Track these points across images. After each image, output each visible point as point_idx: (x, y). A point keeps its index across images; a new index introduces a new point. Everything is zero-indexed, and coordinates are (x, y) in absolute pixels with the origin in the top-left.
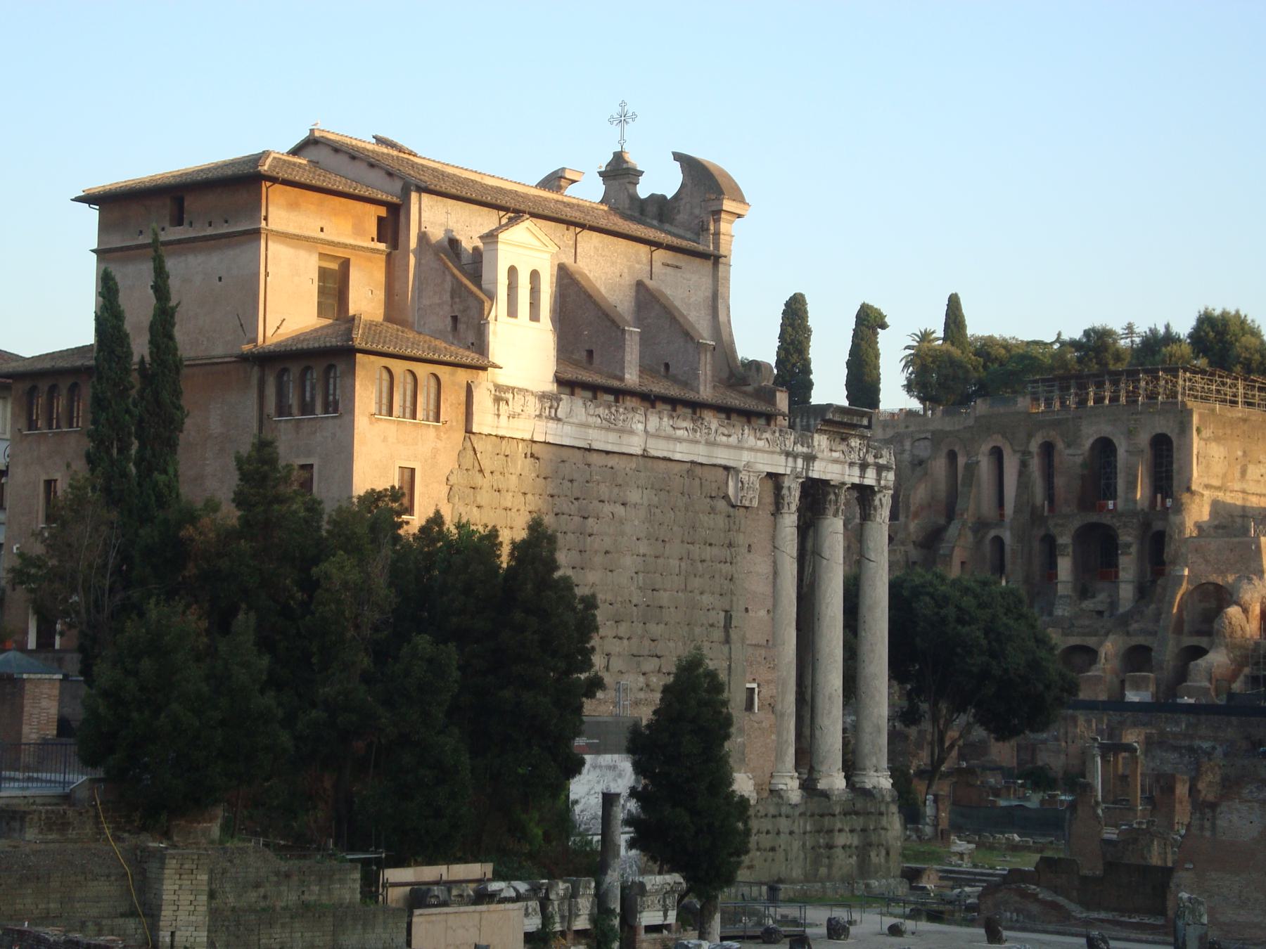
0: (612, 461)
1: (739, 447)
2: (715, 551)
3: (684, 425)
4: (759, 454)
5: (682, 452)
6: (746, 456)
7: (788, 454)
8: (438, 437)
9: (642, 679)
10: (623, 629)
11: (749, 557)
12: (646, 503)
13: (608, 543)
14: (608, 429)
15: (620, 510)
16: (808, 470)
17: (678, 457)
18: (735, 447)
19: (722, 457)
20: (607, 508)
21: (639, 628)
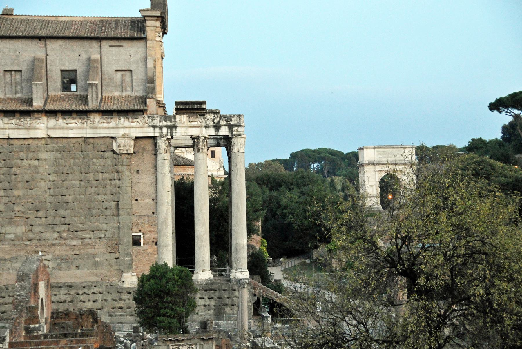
0: (26, 142)
2: (105, 175)
4: (132, 129)
6: (122, 131)
7: (154, 127)
9: (56, 235)
10: (40, 214)
11: (137, 176)
12: (53, 158)
13: (27, 177)
14: (18, 129)
15: (36, 163)
16: (172, 132)
18: (113, 128)
20: (25, 162)
21: (52, 213)
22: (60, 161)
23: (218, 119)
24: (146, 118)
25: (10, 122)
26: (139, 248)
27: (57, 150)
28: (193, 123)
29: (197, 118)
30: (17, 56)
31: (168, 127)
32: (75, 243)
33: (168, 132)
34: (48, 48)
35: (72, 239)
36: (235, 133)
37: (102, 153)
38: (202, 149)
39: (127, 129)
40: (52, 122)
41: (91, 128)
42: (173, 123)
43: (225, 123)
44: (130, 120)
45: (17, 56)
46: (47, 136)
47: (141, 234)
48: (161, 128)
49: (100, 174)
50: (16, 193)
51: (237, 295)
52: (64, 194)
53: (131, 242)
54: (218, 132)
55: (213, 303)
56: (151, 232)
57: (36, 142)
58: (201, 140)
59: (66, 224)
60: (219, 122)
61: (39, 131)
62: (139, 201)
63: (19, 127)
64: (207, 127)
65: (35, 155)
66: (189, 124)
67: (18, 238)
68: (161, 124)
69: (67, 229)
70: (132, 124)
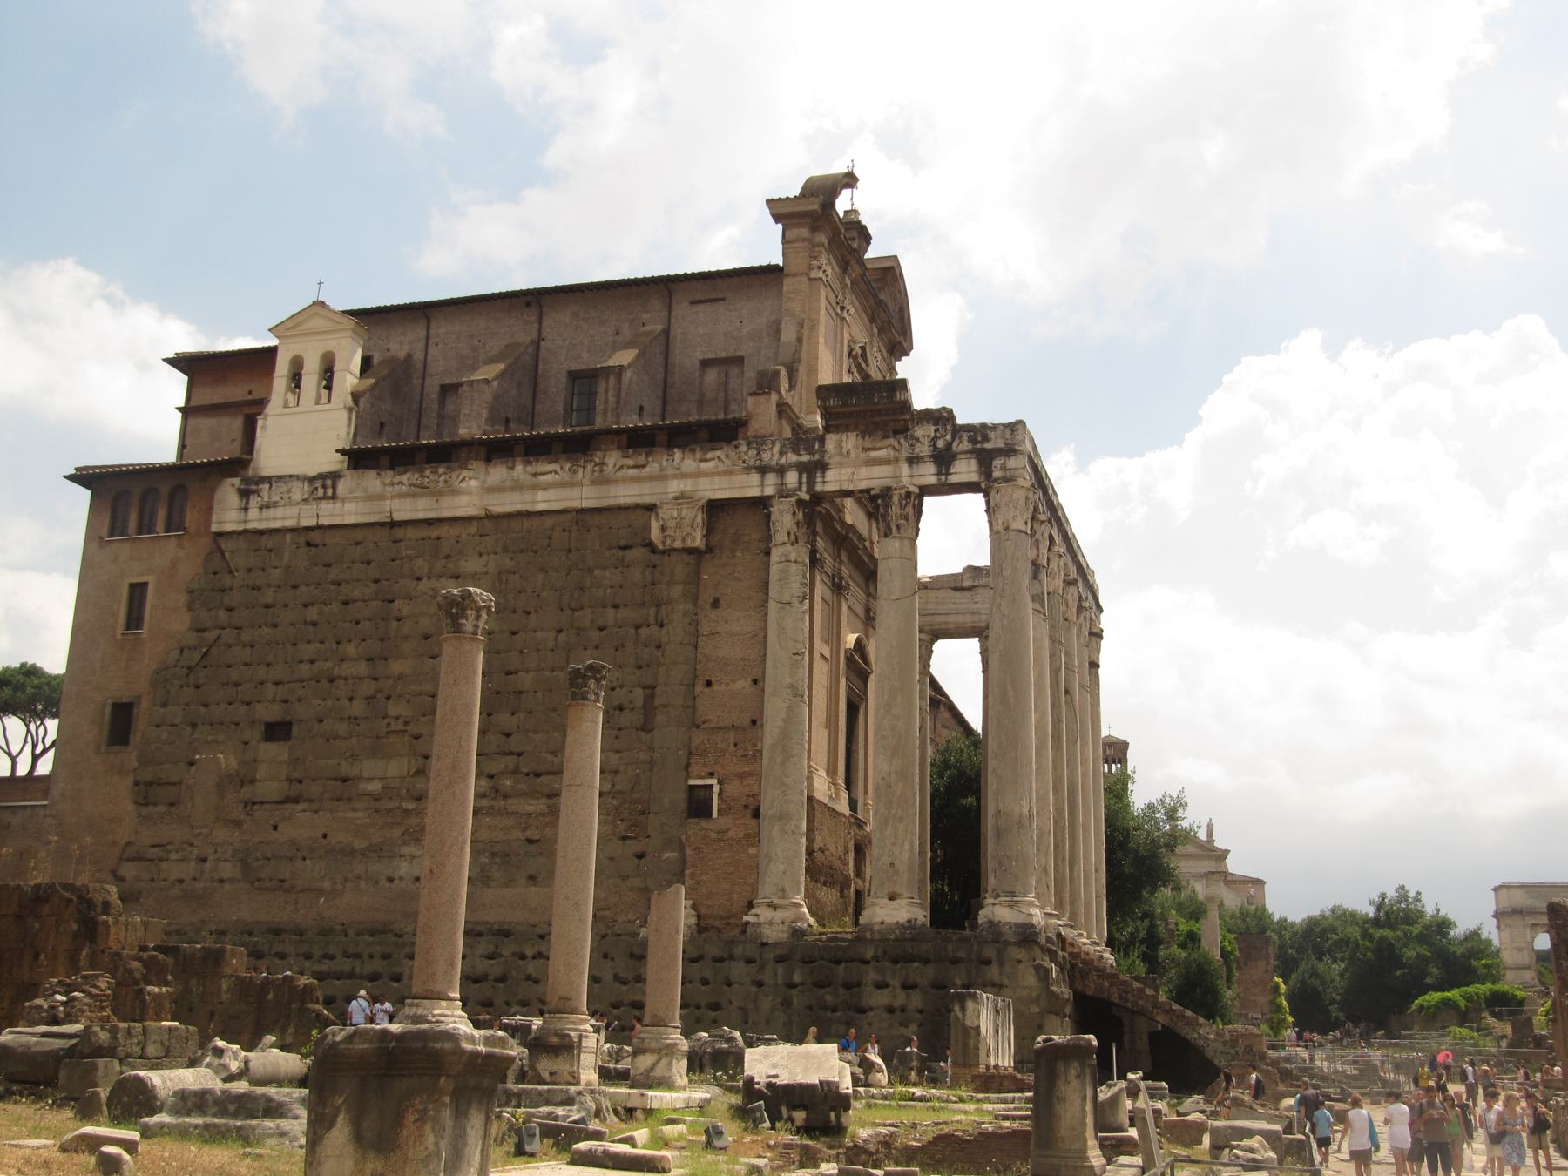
1: (662, 477)
2: (624, 613)
3: (552, 471)
5: (544, 501)
6: (675, 487)
7: (763, 470)
8: (180, 546)
11: (713, 614)
12: (492, 568)
14: (414, 495)
16: (811, 483)
17: (541, 507)
18: (651, 478)
19: (626, 494)
22: (511, 577)
23: (949, 437)
24: (744, 448)
25: (397, 479)
26: (704, 824)
27: (506, 550)
28: (873, 454)
29: (886, 437)
30: (474, 349)
31: (800, 468)
32: (530, 809)
33: (800, 483)
34: (545, 323)
35: (523, 794)
36: (997, 474)
37: (621, 553)
38: (898, 527)
39: (689, 481)
40: (498, 473)
41: (593, 482)
42: (817, 457)
43: (966, 446)
44: (698, 455)
45: (474, 349)
46: (483, 513)
47: (713, 781)
48: (781, 471)
49: (611, 611)
50: (396, 667)
51: (996, 978)
52: (512, 668)
53: (684, 806)
54: (948, 474)
55: (916, 1001)
56: (741, 776)
57: (453, 531)
58: (896, 499)
59: (511, 753)
60: (949, 445)
61: (464, 500)
62: (715, 687)
63: (420, 490)
64: (913, 461)
65: (451, 566)
66: (863, 455)
67: (388, 792)
68: (783, 461)
69: (512, 767)
70: (703, 465)
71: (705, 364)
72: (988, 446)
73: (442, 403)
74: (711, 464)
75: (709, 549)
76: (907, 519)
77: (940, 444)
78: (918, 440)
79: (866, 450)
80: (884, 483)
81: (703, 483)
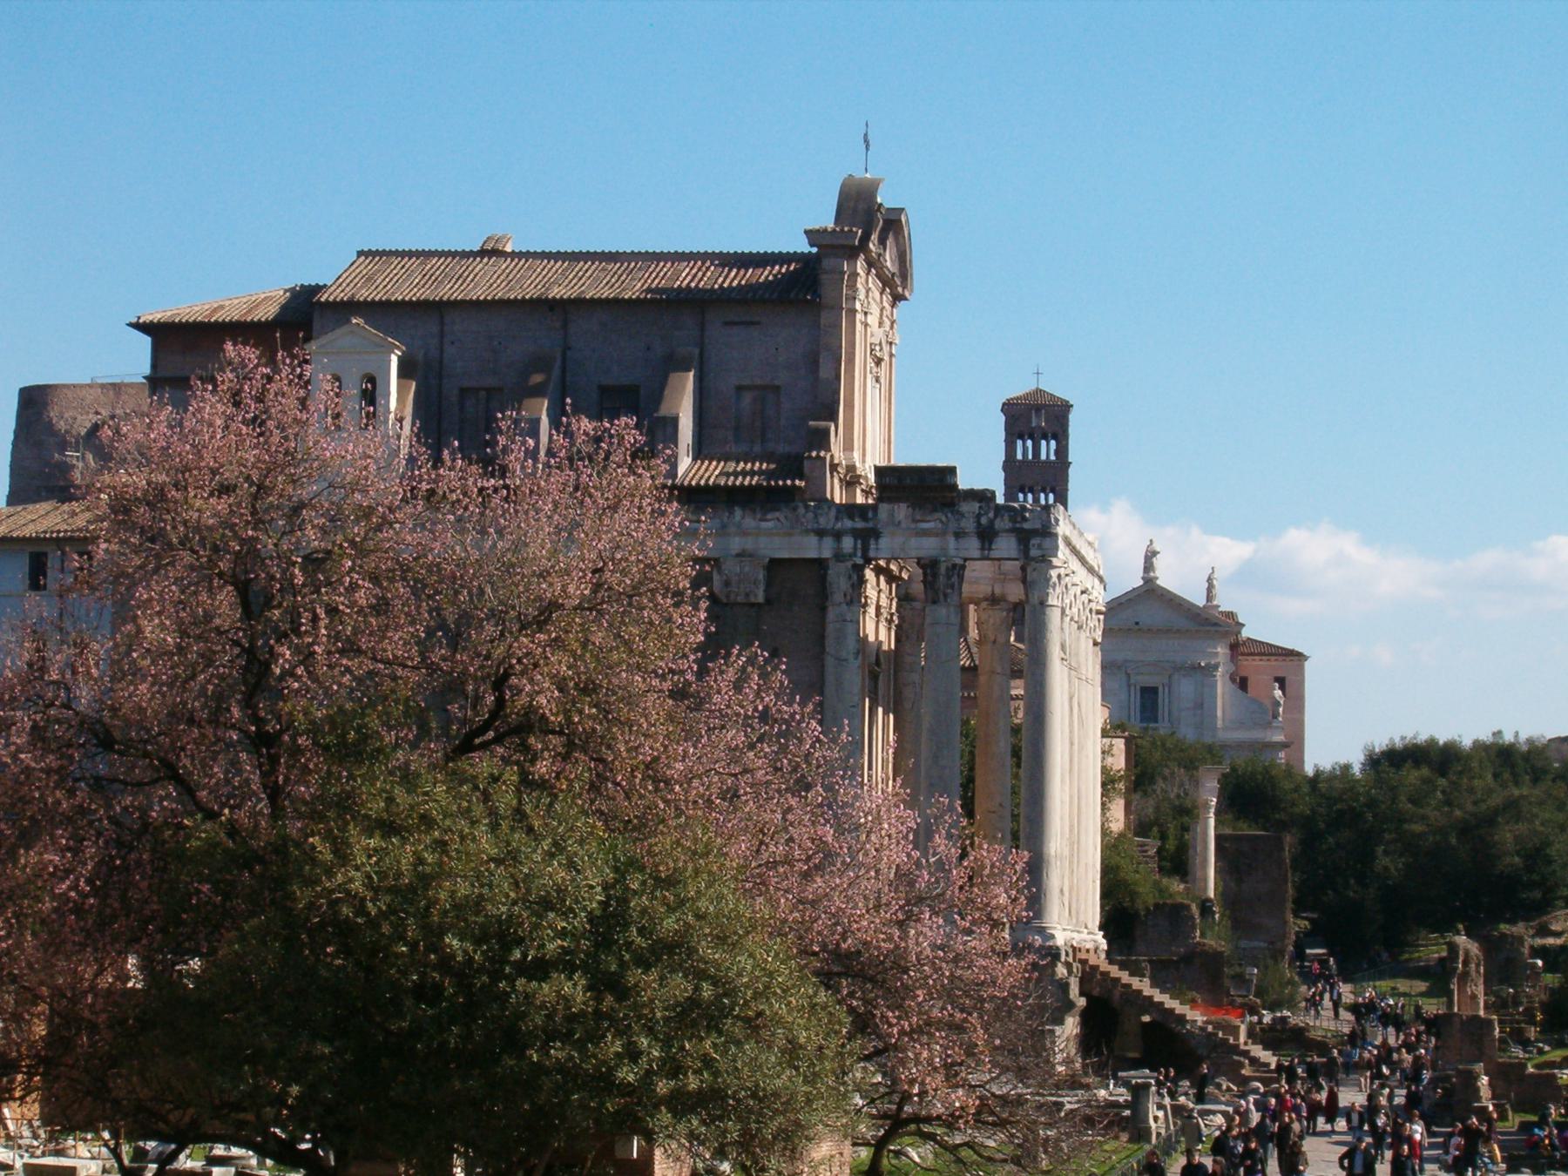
6: (736, 544)
7: (821, 533)
16: (865, 550)
23: (991, 515)
29: (935, 510)
31: (856, 534)
33: (855, 548)
42: (870, 525)
60: (992, 522)
64: (959, 535)
68: (839, 525)
70: (764, 525)
71: (740, 389)
72: (1026, 526)
73: (462, 409)
74: (770, 524)
75: (768, 601)
76: (952, 587)
77: (984, 521)
78: (963, 515)
79: (915, 521)
80: (933, 553)
81: (763, 541)
